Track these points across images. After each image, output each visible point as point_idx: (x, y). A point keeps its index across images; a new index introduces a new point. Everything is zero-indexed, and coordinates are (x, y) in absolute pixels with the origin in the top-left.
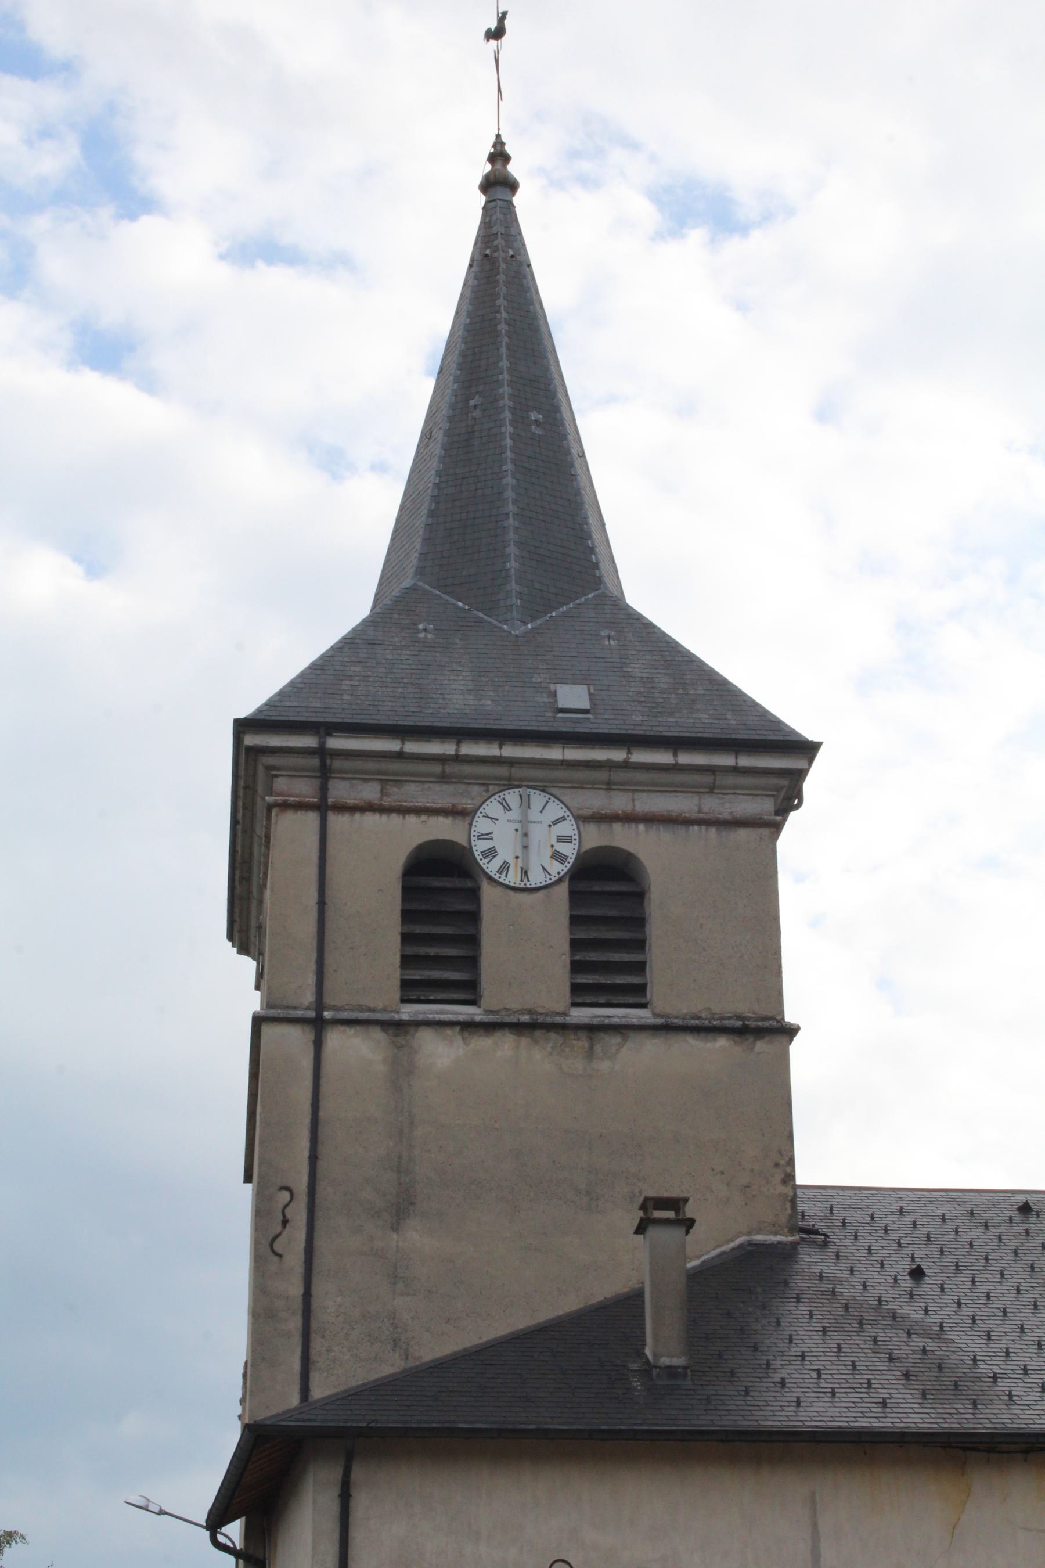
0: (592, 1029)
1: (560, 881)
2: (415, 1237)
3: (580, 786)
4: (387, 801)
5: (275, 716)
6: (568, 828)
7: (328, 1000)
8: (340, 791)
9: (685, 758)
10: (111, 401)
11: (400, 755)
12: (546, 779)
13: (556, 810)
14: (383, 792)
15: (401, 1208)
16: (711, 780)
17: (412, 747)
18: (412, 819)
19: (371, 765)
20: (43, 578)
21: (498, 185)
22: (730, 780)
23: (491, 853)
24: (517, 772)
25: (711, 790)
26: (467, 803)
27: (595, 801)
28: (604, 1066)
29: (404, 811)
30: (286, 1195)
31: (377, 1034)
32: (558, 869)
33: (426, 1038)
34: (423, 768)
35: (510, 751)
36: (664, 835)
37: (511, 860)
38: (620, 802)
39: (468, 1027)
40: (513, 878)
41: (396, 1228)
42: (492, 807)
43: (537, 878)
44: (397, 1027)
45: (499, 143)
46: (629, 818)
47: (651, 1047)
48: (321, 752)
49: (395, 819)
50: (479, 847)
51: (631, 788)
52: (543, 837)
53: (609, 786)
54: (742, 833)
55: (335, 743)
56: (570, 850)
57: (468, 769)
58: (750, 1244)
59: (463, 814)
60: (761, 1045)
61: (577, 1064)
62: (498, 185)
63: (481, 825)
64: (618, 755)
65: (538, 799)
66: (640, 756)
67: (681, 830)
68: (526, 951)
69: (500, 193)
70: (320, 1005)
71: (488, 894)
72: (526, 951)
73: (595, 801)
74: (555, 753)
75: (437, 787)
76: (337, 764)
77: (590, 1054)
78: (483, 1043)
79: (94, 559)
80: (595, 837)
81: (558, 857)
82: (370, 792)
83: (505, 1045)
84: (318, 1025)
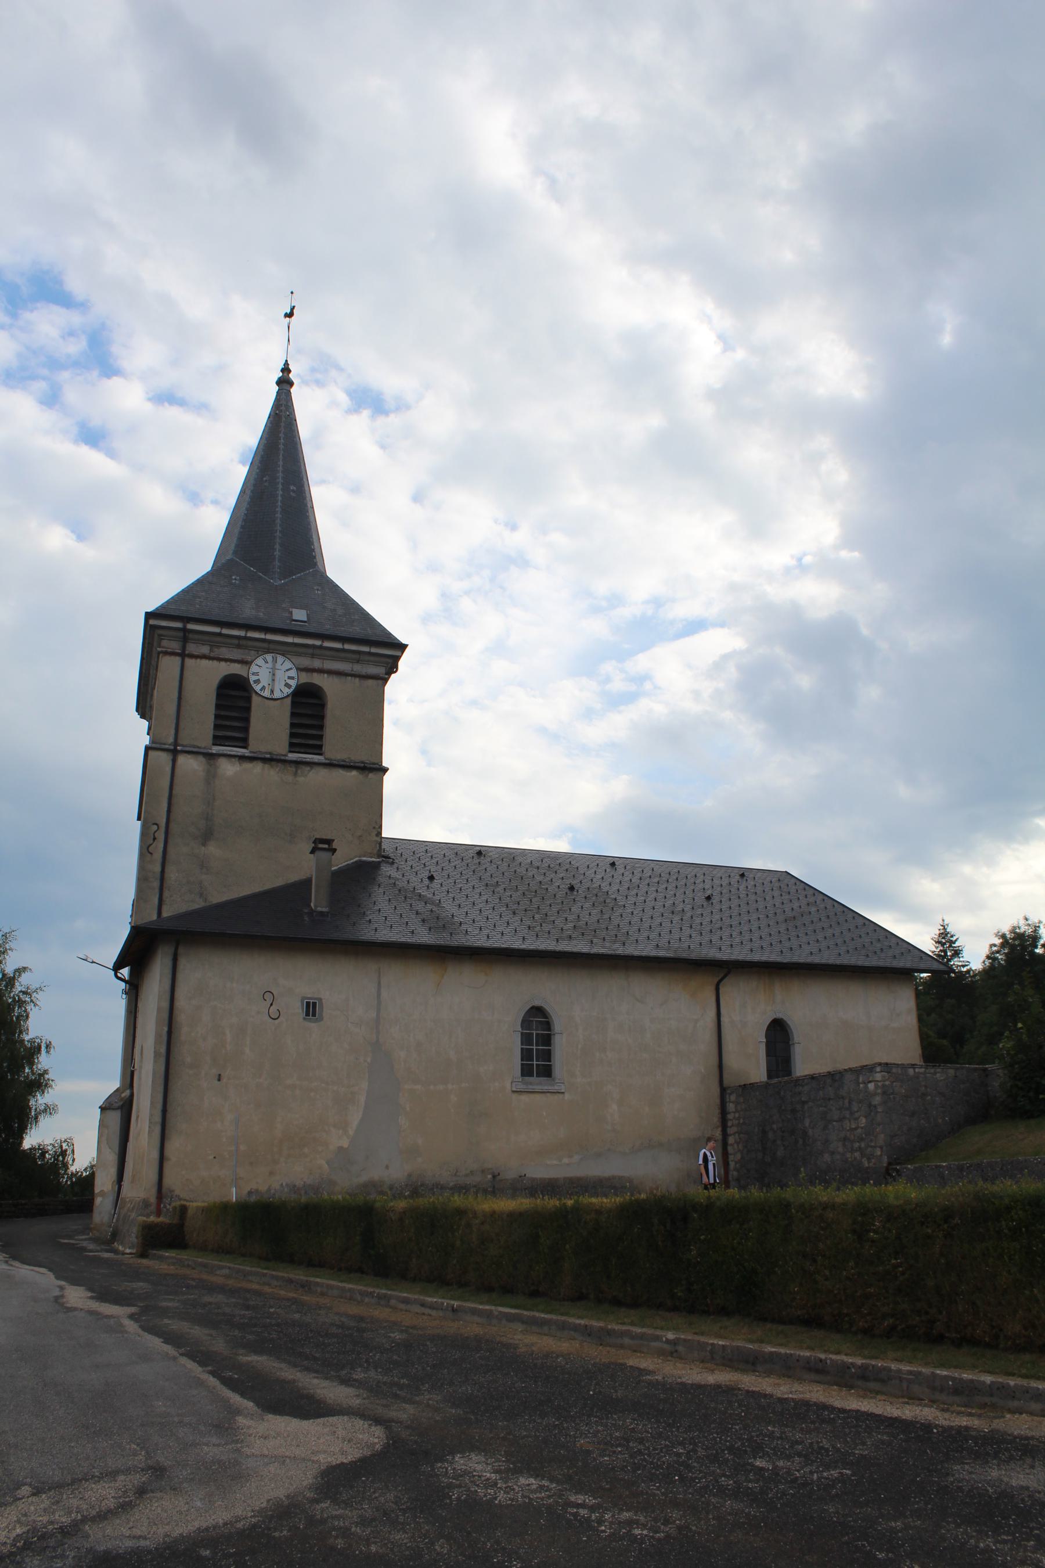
0: (298, 763)
1: (288, 696)
2: (212, 849)
3: (300, 655)
4: (212, 655)
5: (164, 612)
6: (293, 673)
7: (180, 742)
8: (191, 648)
9: (347, 647)
10: (95, 461)
11: (220, 634)
12: (285, 650)
13: (288, 664)
14: (211, 651)
15: (206, 836)
16: (358, 657)
17: (225, 631)
18: (223, 664)
19: (207, 638)
20: (56, 539)
21: (285, 382)
22: (367, 658)
23: (257, 682)
24: (272, 646)
25: (358, 661)
26: (249, 659)
27: (306, 662)
28: (301, 779)
29: (220, 660)
30: (155, 827)
31: (201, 758)
32: (287, 691)
35: (269, 637)
36: (336, 680)
37: (266, 685)
38: (317, 664)
39: (242, 758)
40: (266, 693)
41: (204, 844)
42: (260, 661)
43: (277, 694)
44: (211, 757)
45: (286, 363)
46: (321, 671)
47: (323, 772)
48: (184, 630)
49: (215, 662)
50: (252, 678)
51: (322, 657)
52: (281, 676)
53: (313, 656)
54: (370, 682)
55: (190, 626)
56: (293, 683)
57: (250, 643)
58: (360, 861)
59: (248, 663)
60: (371, 775)
61: (290, 778)
62: (285, 382)
63: (254, 668)
64: (318, 643)
65: (280, 659)
66: (328, 644)
67: (343, 679)
68: (270, 728)
69: (285, 386)
70: (176, 743)
71: (255, 698)
72: (270, 728)
73: (306, 662)
74: (289, 639)
75: (235, 650)
76: (191, 636)
77: (295, 774)
78: (248, 766)
79: (81, 531)
80: (305, 678)
81: (287, 685)
82: (205, 650)
83: (257, 768)
84: (174, 753)
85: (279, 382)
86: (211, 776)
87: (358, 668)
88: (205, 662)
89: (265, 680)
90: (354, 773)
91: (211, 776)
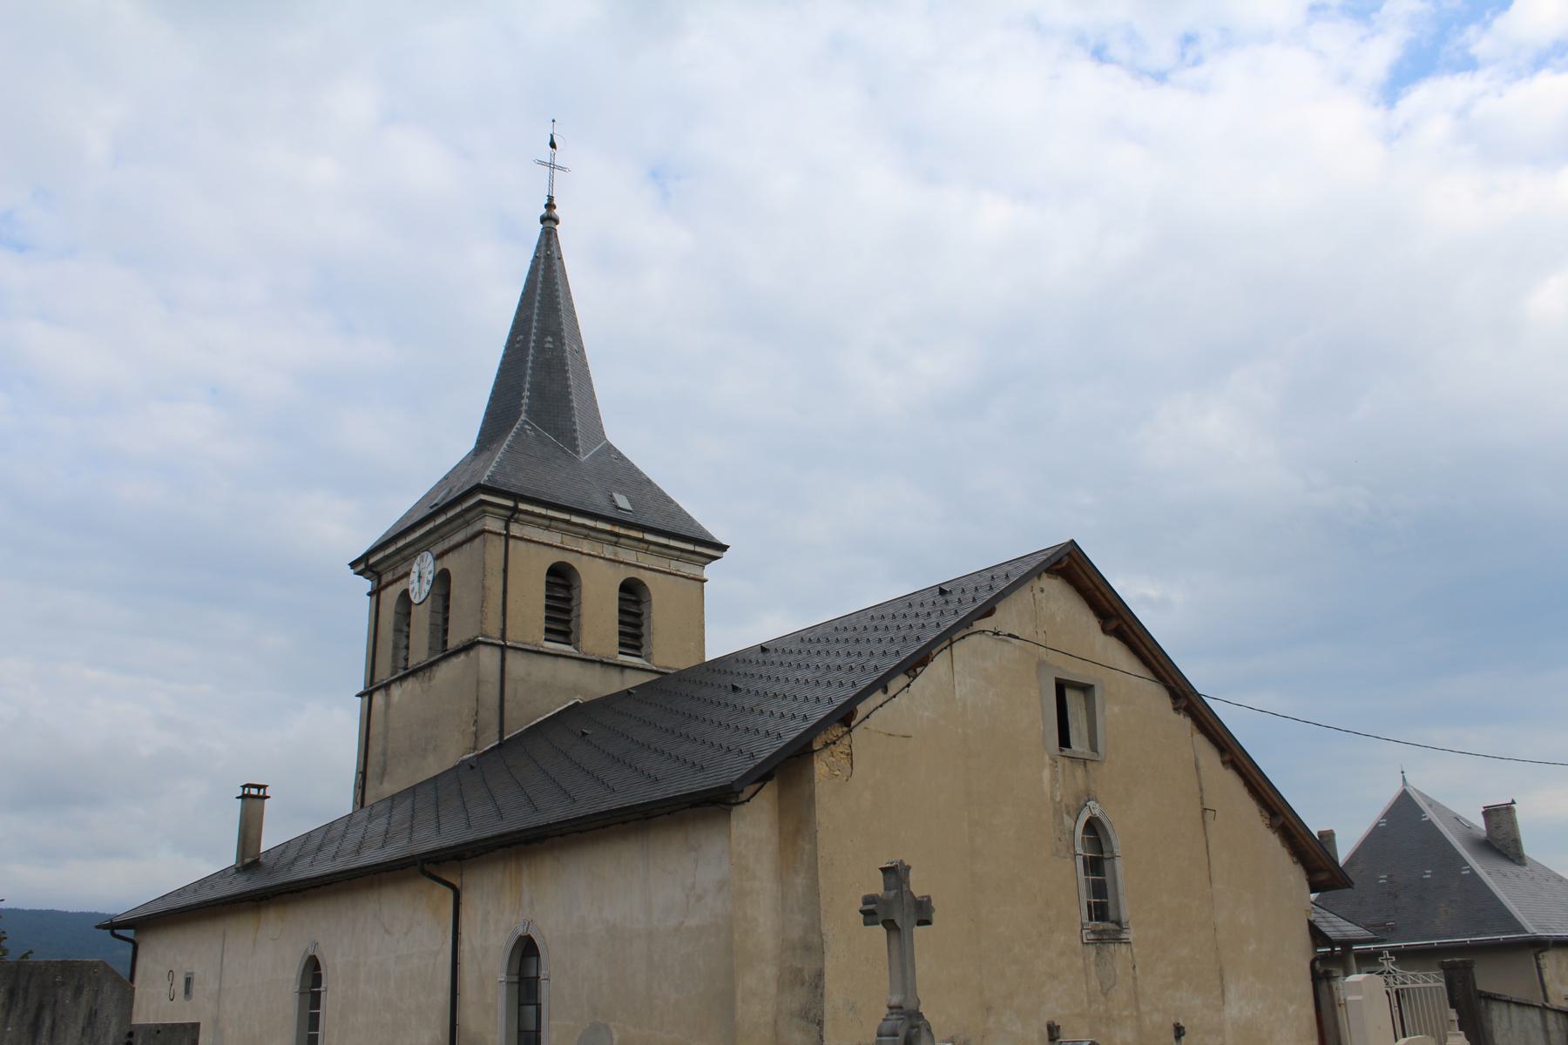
3: (435, 543)
8: (387, 578)
9: (451, 514)
21: (549, 220)
28: (433, 682)
31: (383, 691)
33: (393, 687)
34: (539, 521)
35: (409, 539)
45: (551, 198)
55: (371, 561)
56: (430, 578)
59: (407, 574)
60: (472, 653)
62: (549, 220)
69: (548, 224)
76: (379, 568)
78: (405, 684)
85: (543, 220)
86: (388, 704)
87: (470, 531)
88: (390, 589)
89: (416, 585)
90: (462, 657)
91: (388, 704)
